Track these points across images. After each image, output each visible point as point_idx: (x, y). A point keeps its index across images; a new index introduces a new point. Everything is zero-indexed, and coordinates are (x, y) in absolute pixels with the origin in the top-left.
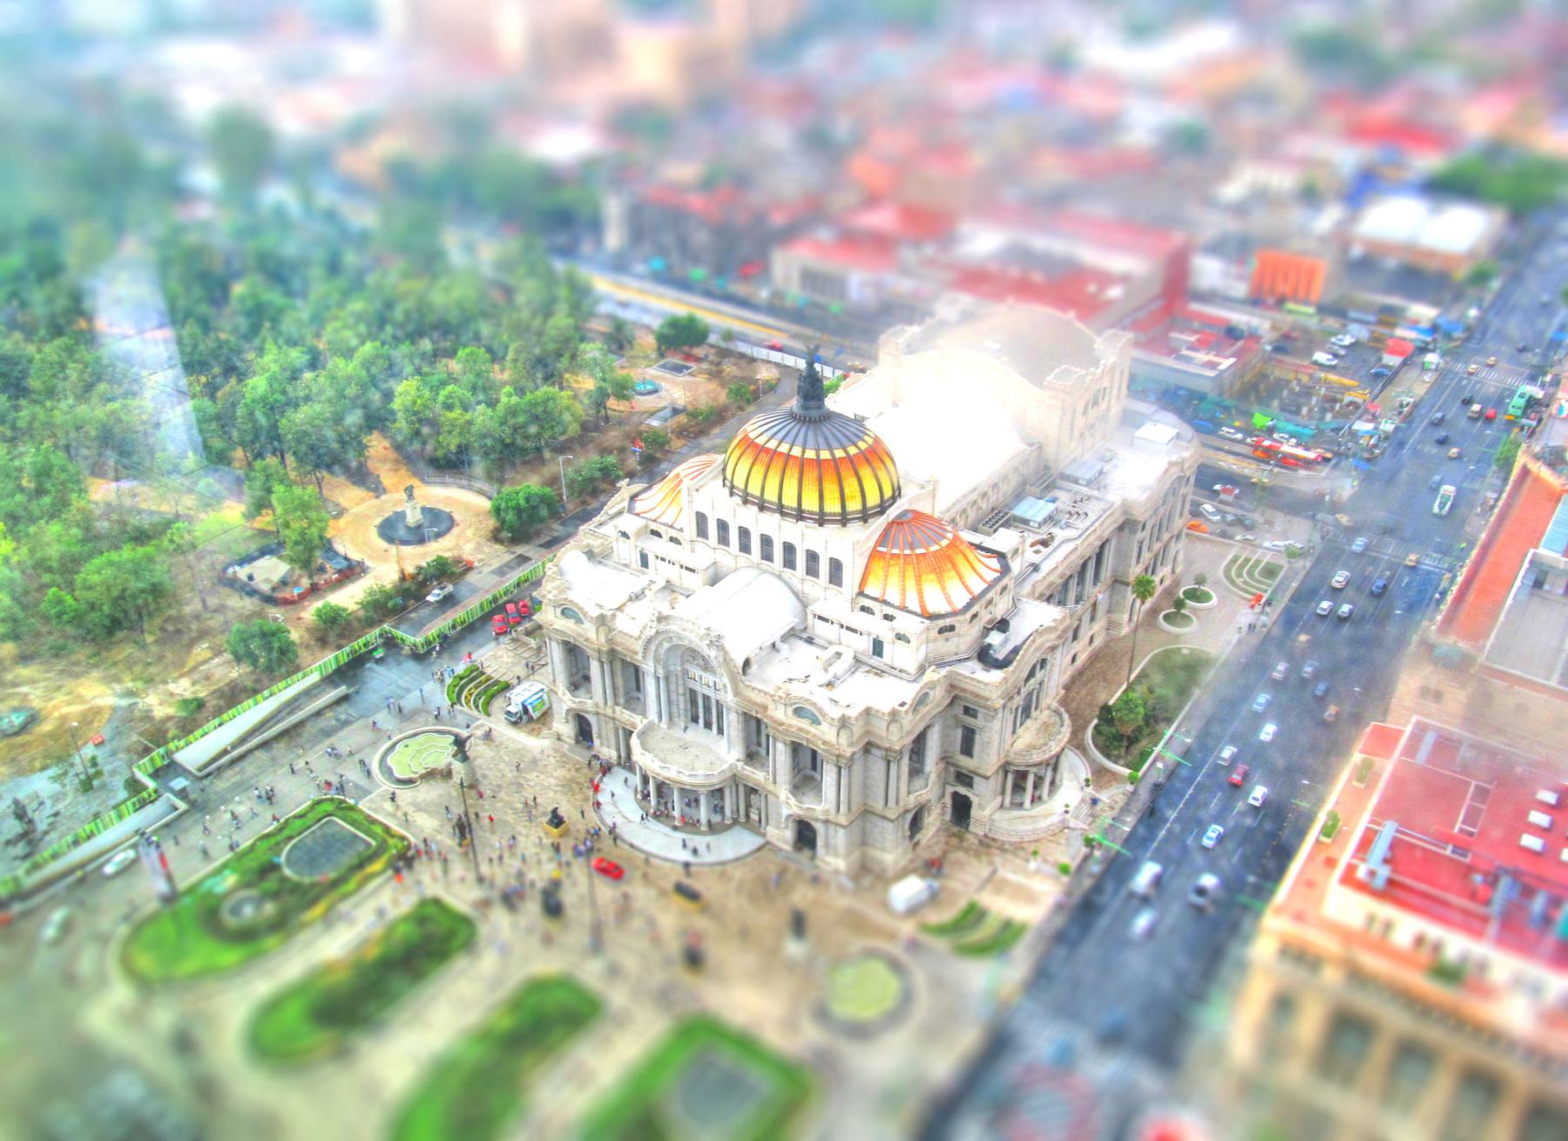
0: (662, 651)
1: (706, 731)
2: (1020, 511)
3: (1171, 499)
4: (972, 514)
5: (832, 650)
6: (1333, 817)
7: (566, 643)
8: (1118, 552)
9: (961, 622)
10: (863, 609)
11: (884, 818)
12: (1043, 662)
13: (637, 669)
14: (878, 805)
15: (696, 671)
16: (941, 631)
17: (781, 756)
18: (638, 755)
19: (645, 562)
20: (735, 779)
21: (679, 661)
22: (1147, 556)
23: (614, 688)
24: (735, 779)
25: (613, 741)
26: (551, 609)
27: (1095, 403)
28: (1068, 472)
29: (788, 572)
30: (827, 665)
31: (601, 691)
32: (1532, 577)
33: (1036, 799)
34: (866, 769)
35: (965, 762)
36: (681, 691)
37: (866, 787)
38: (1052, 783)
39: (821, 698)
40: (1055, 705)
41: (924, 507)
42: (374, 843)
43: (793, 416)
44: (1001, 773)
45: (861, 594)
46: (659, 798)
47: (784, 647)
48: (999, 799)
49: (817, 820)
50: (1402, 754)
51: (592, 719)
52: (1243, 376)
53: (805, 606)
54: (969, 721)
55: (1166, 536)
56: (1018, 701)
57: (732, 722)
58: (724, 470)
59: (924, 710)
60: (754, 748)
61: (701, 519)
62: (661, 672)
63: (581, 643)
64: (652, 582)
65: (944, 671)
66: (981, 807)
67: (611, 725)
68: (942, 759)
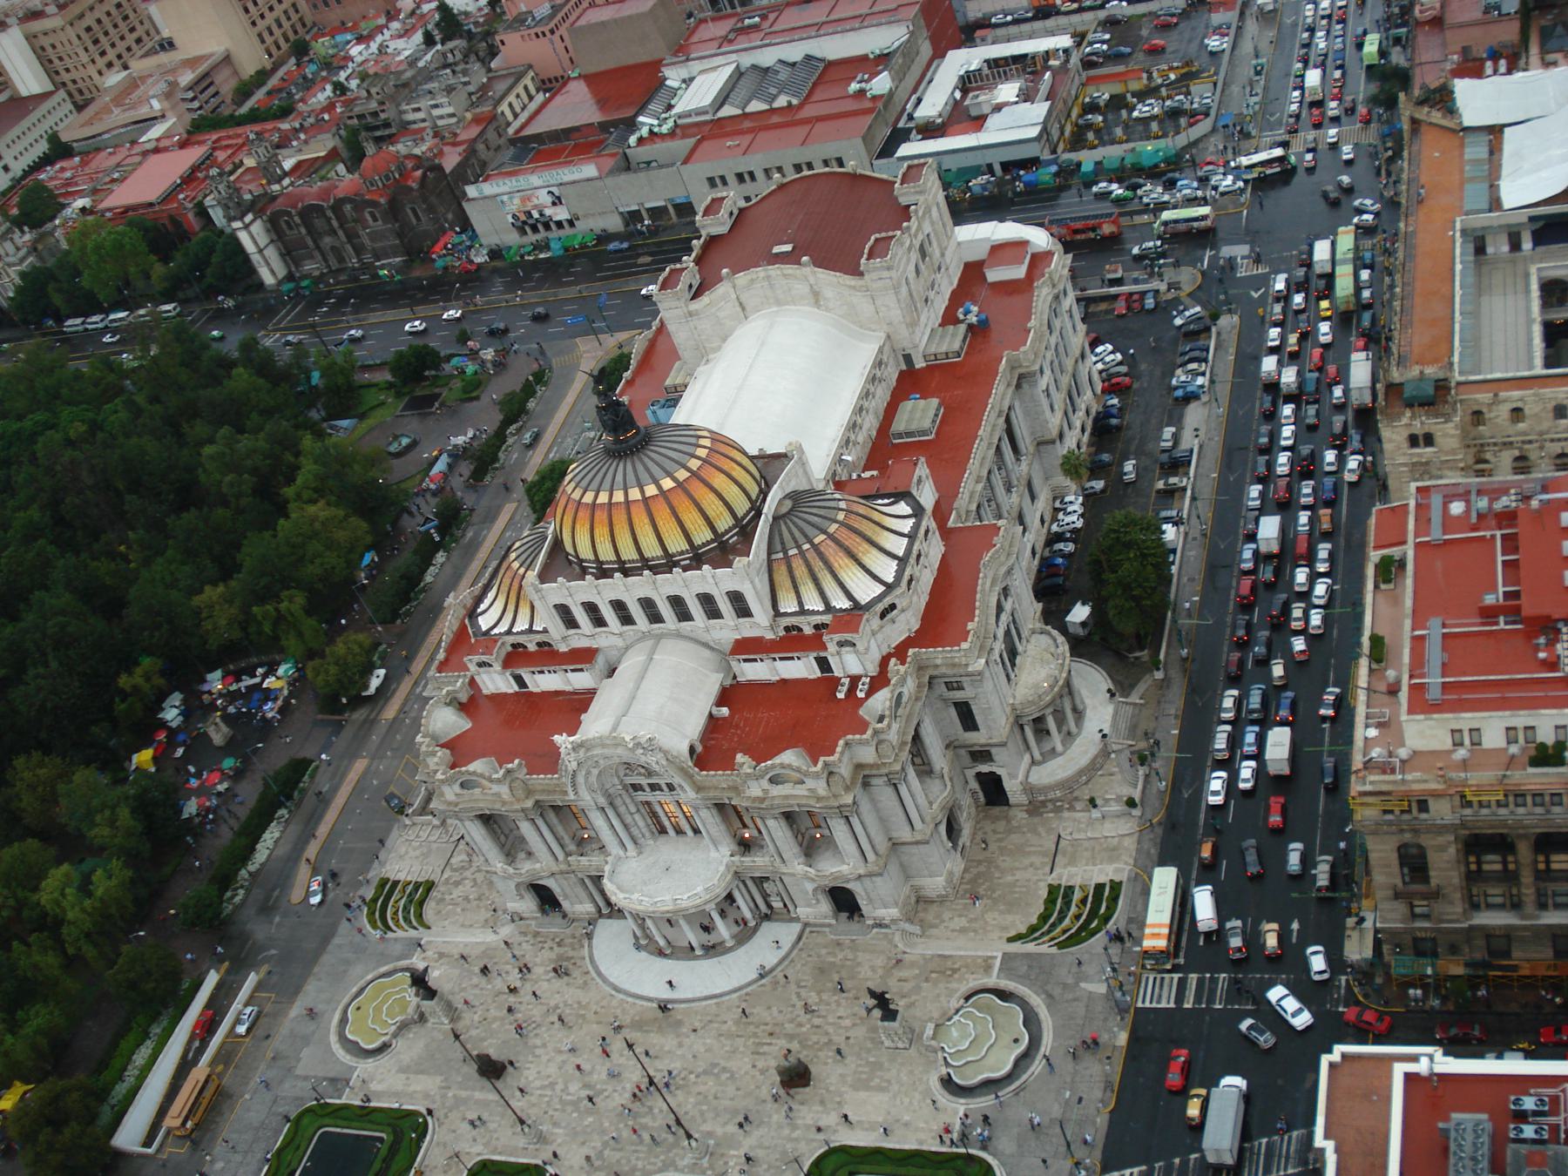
0: (593, 779)
1: (681, 838)
3: (1057, 324)
6: (1376, 641)
8: (1027, 413)
12: (1005, 591)
14: (905, 834)
16: (883, 616)
17: (777, 831)
18: (618, 898)
21: (616, 781)
22: (1059, 398)
23: (558, 839)
25: (583, 894)
28: (932, 350)
29: (686, 626)
31: (544, 849)
32: (1471, 248)
33: (1069, 736)
34: (873, 801)
36: (633, 809)
37: (883, 821)
38: (1075, 710)
40: (1039, 625)
42: (384, 1135)
44: (1017, 730)
45: (778, 614)
47: (725, 711)
48: (1027, 757)
50: (1416, 536)
51: (550, 883)
52: (1069, 115)
56: (999, 646)
57: (708, 820)
61: (564, 612)
62: (602, 801)
63: (497, 808)
66: (1013, 776)
68: (947, 747)
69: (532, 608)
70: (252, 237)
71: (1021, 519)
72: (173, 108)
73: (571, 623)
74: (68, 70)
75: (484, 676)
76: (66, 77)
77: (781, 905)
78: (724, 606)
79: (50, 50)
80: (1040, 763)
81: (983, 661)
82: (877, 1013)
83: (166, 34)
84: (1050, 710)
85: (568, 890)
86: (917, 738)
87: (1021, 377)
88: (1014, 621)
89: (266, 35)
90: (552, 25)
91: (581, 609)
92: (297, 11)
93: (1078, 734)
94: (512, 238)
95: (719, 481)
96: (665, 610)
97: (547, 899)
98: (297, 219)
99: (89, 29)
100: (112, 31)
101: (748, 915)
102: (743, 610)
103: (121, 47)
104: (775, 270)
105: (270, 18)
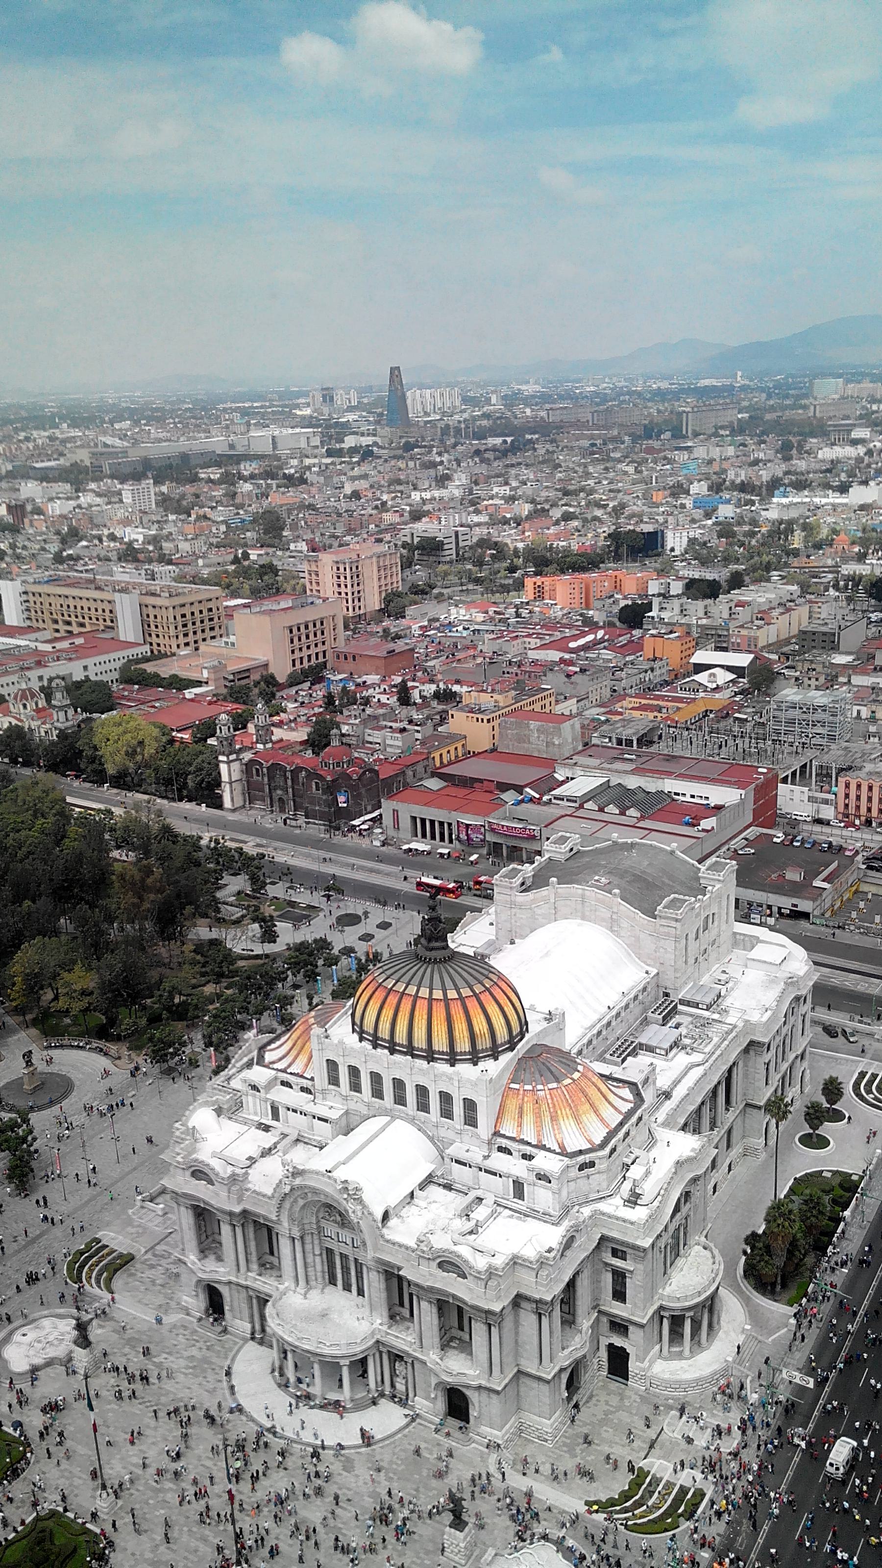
0: (297, 1209)
2: (643, 1039)
3: (792, 1020)
7: (195, 1208)
10: (500, 1149)
11: (539, 1379)
12: (686, 1195)
13: (269, 1230)
17: (427, 1313)
19: (276, 1116)
22: (775, 1079)
28: (688, 997)
31: (233, 1256)
34: (517, 1323)
35: (618, 1309)
36: (317, 1252)
38: (710, 1326)
39: (464, 1251)
40: (703, 1239)
44: (656, 1319)
45: (497, 1134)
46: (299, 1371)
48: (658, 1347)
49: (468, 1387)
51: (224, 1290)
54: (618, 1263)
56: (667, 1238)
57: (374, 1282)
61: (332, 1065)
62: (296, 1234)
64: (285, 1136)
69: (311, 1057)
70: (229, 771)
72: (215, 680)
73: (334, 1080)
74: (158, 636)
75: (250, 1098)
76: (154, 640)
77: (403, 1388)
78: (458, 1109)
79: (152, 617)
80: (666, 1359)
81: (651, 1241)
84: (692, 1314)
85: (236, 1304)
87: (752, 1043)
88: (685, 1228)
89: (298, 662)
90: (490, 717)
91: (346, 1069)
92: (324, 657)
93: (707, 1348)
98: (265, 770)
99: (183, 616)
100: (198, 623)
102: (471, 1120)
104: (591, 893)
105: (305, 653)
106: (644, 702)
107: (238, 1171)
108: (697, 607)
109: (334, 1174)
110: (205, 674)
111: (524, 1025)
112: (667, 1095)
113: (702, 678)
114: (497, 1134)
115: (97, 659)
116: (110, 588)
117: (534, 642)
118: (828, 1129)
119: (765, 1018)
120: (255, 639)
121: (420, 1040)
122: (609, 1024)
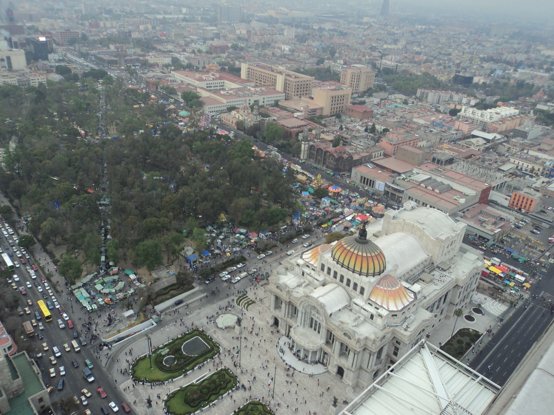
2: (422, 277)
3: (472, 279)
4: (407, 276)
5: (358, 315)
9: (399, 314)
10: (369, 304)
12: (423, 330)
13: (296, 308)
14: (365, 367)
15: (313, 312)
16: (393, 316)
17: (337, 345)
18: (292, 334)
20: (321, 349)
22: (462, 296)
23: (288, 312)
24: (321, 349)
25: (285, 328)
26: (273, 285)
27: (451, 244)
30: (356, 319)
31: (284, 312)
34: (363, 355)
41: (392, 274)
43: (356, 240)
53: (351, 299)
55: (469, 290)
57: (323, 331)
58: (332, 251)
59: (384, 340)
60: (329, 340)
62: (304, 311)
64: (305, 282)
65: (391, 329)
67: (285, 323)
71: (436, 316)
73: (323, 269)
76: (287, 92)
78: (359, 289)
82: (333, 403)
83: (313, 96)
86: (382, 348)
87: (457, 285)
94: (358, 182)
95: (376, 262)
96: (345, 281)
97: (276, 322)
99: (298, 85)
101: (317, 359)
103: (302, 93)
106: (450, 147)
107: (290, 290)
108: (479, 112)
109: (319, 299)
110: (302, 109)
111: (385, 268)
112: (425, 298)
113: (473, 140)
114: (369, 299)
115: (268, 96)
116: (275, 71)
117: (416, 115)
118: (475, 315)
119: (463, 278)
120: (321, 98)
121: (351, 266)
122: (412, 270)
